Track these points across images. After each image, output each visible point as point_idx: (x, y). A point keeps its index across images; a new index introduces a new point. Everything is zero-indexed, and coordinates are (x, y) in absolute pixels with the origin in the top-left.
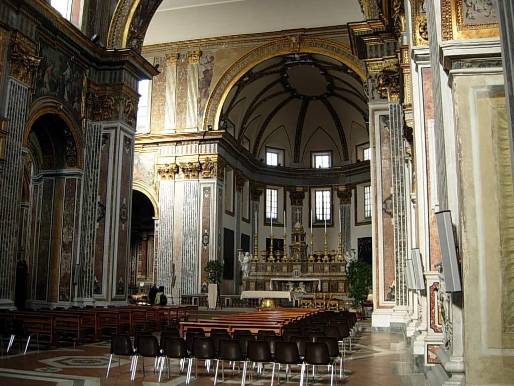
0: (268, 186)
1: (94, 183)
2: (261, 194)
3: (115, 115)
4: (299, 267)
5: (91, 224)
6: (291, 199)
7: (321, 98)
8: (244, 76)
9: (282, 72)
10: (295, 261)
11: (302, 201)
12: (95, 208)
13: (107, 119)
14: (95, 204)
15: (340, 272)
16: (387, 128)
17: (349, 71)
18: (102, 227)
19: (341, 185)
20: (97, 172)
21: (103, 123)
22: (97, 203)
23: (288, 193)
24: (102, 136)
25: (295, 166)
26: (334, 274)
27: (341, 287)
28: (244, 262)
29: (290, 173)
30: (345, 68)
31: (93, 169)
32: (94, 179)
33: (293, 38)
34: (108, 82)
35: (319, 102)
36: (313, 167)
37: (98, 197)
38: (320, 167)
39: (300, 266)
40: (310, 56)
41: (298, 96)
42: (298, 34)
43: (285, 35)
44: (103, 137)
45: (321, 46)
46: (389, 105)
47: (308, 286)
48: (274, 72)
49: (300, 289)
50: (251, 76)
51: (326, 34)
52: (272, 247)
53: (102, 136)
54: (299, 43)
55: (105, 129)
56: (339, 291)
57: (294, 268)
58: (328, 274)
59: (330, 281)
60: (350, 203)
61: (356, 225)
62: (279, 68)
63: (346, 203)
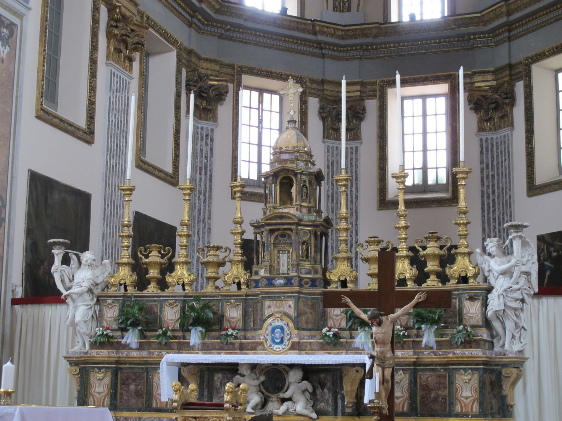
0: (247, 79)
2: (220, 96)
4: (289, 306)
6: (323, 119)
10: (270, 282)
11: (359, 128)
19: (480, 73)
27: (466, 393)
28: (75, 290)
29: (320, 38)
36: (394, 18)
38: (412, 17)
39: (291, 303)
47: (323, 387)
49: (290, 399)
56: (458, 409)
57: (267, 313)
59: (415, 364)
60: (512, 124)
63: (496, 128)
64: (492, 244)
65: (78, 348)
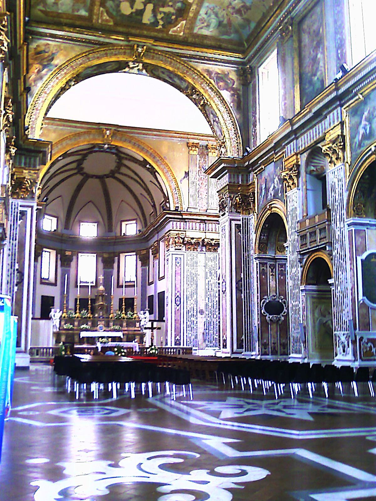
0: (44, 249)
1: (12, 253)
3: (30, 196)
5: (10, 288)
7: (101, 178)
8: (60, 157)
9: (85, 156)
12: (14, 274)
13: (24, 198)
14: (14, 271)
15: (135, 327)
16: (239, 233)
17: (148, 166)
18: (21, 290)
20: (16, 243)
21: (21, 202)
22: (16, 270)
23: (59, 256)
24: (19, 212)
25: (65, 232)
26: (131, 329)
30: (144, 163)
31: (11, 240)
32: (12, 249)
33: (108, 132)
34: (23, 165)
35: (97, 181)
37: (17, 265)
40: (117, 148)
41: (82, 174)
42: (113, 128)
43: (101, 127)
44: (20, 213)
45: (130, 142)
46: (241, 218)
48: (80, 154)
50: (65, 155)
51: (132, 133)
52: (124, 307)
53: (19, 212)
54: (112, 137)
55: (21, 206)
58: (126, 329)
61: (117, 287)
62: (85, 152)
63: (110, 268)
64: (142, 312)
65: (55, 330)
